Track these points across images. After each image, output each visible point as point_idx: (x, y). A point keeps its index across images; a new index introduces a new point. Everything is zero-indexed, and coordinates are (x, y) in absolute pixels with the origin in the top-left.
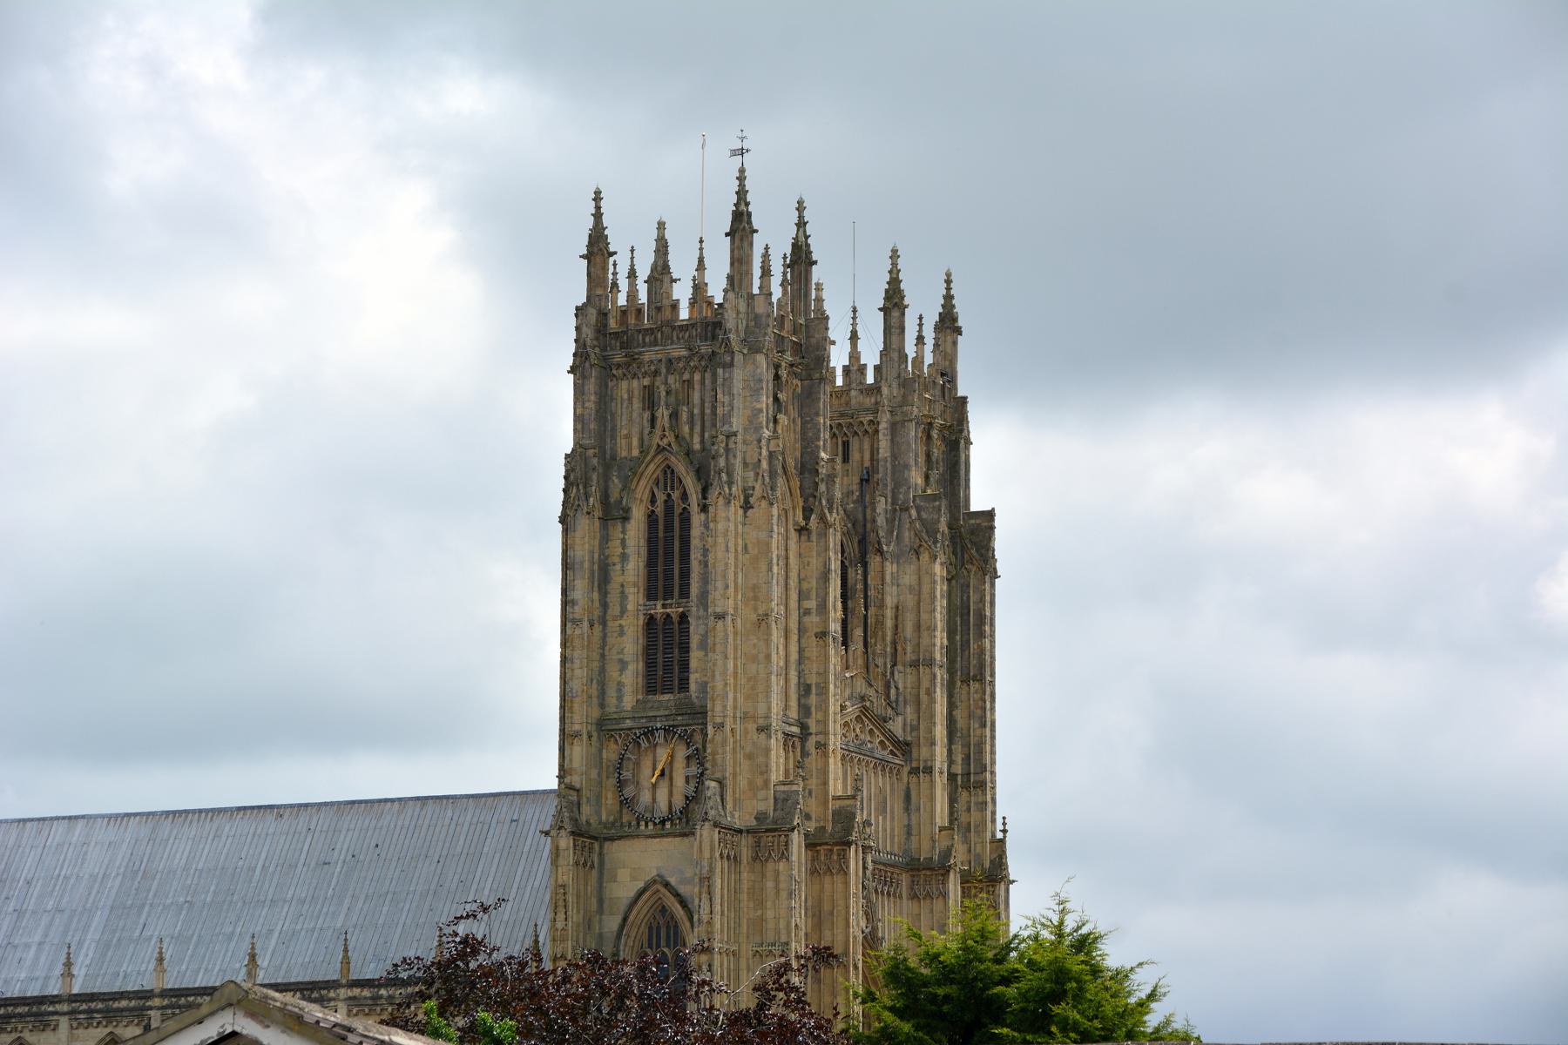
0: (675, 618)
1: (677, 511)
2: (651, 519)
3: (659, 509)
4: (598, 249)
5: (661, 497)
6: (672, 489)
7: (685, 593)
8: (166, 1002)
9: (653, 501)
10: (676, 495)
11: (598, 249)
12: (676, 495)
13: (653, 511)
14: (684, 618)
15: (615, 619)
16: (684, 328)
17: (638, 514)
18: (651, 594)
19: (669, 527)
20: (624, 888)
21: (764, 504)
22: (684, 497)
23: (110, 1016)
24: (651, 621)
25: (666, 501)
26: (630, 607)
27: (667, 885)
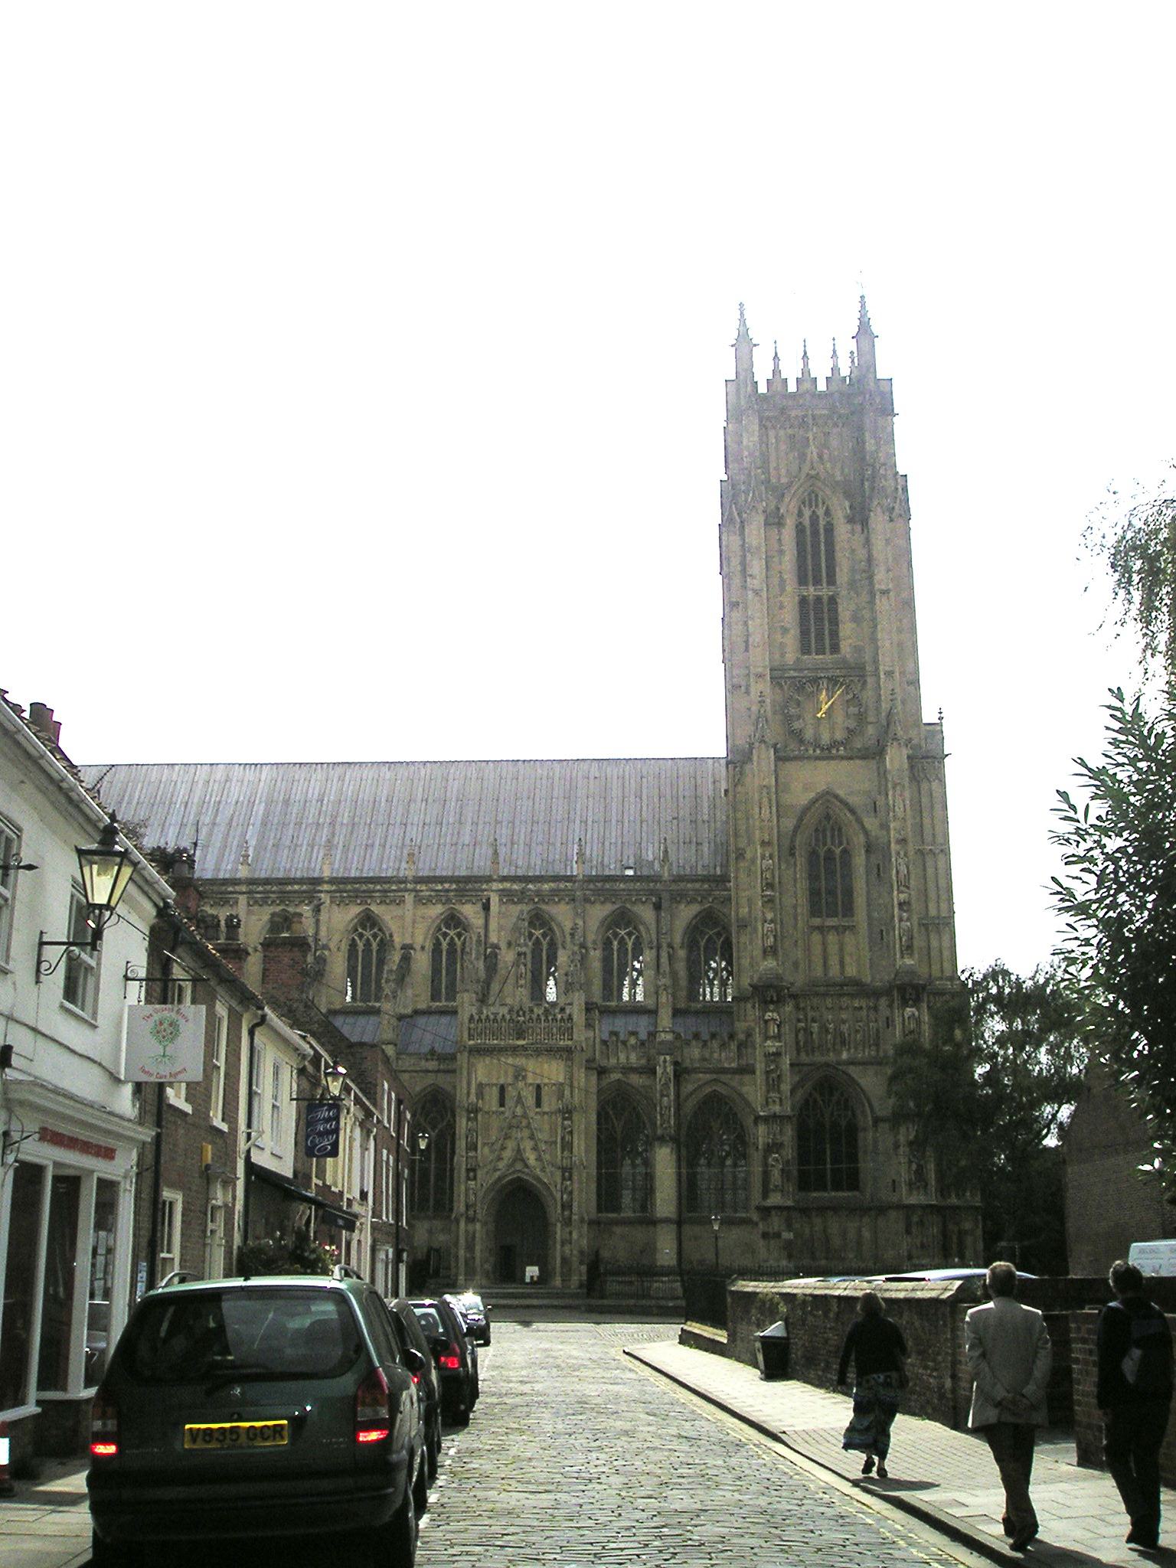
0: (825, 599)
1: (822, 523)
2: (800, 529)
3: (807, 522)
4: (744, 344)
5: (807, 513)
6: (817, 506)
7: (832, 580)
8: (334, 888)
9: (800, 514)
10: (821, 512)
11: (744, 344)
12: (821, 512)
13: (800, 523)
14: (833, 600)
15: (775, 597)
16: (822, 395)
17: (790, 522)
18: (802, 580)
19: (815, 533)
20: (799, 796)
21: (900, 520)
22: (827, 513)
23: (284, 897)
24: (803, 601)
25: (811, 517)
26: (789, 589)
27: (836, 797)
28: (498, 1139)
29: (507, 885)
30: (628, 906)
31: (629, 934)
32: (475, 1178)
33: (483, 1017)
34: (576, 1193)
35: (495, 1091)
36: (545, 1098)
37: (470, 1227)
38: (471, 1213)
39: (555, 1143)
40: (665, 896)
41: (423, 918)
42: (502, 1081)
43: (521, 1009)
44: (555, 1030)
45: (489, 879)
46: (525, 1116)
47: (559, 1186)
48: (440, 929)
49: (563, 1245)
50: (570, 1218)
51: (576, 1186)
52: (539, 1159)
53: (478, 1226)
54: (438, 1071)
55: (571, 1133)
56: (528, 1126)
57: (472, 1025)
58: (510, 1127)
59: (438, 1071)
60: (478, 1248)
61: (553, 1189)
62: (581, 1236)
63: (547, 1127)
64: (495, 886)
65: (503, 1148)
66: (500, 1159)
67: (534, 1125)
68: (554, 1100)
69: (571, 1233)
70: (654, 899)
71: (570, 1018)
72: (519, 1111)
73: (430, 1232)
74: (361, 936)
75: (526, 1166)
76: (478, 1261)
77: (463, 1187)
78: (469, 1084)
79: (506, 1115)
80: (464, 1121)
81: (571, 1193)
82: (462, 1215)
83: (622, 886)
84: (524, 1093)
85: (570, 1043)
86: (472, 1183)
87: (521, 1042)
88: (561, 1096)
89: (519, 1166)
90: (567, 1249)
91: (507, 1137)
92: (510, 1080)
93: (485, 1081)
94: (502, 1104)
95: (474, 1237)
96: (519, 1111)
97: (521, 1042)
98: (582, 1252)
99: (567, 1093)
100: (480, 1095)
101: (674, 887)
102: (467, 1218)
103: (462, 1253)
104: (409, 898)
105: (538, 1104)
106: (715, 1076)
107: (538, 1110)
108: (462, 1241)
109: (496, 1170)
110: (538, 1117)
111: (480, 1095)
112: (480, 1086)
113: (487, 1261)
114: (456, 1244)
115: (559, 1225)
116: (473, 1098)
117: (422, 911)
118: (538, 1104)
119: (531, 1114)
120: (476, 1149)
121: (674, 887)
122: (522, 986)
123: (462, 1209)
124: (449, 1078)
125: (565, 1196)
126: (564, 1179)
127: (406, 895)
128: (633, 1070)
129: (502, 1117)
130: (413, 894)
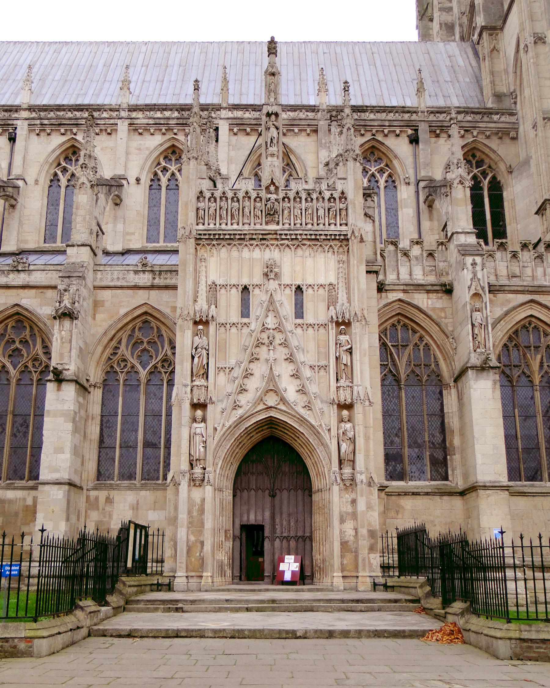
28: (239, 363)
29: (239, 114)
30: (380, 137)
31: (381, 171)
32: (204, 420)
33: (218, 194)
34: (360, 442)
35: (235, 295)
36: (308, 306)
37: (197, 494)
38: (198, 470)
39: (325, 367)
40: (423, 129)
41: (139, 149)
42: (245, 281)
43: (273, 183)
44: (321, 212)
45: (218, 108)
46: (279, 329)
47: (334, 432)
48: (159, 164)
49: (342, 521)
50: (353, 479)
51: (360, 430)
52: (302, 391)
53: (209, 489)
54: (152, 287)
55: (350, 351)
56: (285, 344)
57: (201, 205)
58: (259, 344)
59: (152, 287)
60: (208, 525)
61: (325, 436)
62: (369, 507)
63: (312, 346)
64: (224, 113)
65: (248, 375)
66: (243, 390)
67: (294, 342)
68: (322, 307)
69: (354, 502)
70: (410, 132)
71: (343, 196)
72: (271, 322)
73: (135, 508)
74: (65, 170)
75: (283, 400)
76: (208, 547)
77: (185, 433)
78: (197, 283)
79: (253, 327)
80: (189, 334)
81: (353, 441)
82: (183, 473)
83: (372, 116)
84: (277, 297)
85: (344, 228)
86: (199, 427)
87: (273, 227)
88: (332, 302)
89: (272, 400)
90: (349, 526)
91: (254, 359)
92: (258, 279)
93: (220, 281)
94: (245, 312)
95: (202, 511)
96: (271, 322)
97: (273, 227)
98: (372, 534)
99: (342, 296)
100: (213, 300)
101: (432, 118)
102: (192, 480)
103: (182, 533)
104: (123, 127)
105: (299, 313)
106: (528, 297)
107: (299, 321)
108: (183, 516)
109: (236, 406)
110: (299, 331)
111: (213, 300)
112: (213, 288)
113: (220, 546)
114: (174, 521)
115: (336, 488)
116: (202, 304)
117: (137, 141)
118: (299, 313)
119: (289, 326)
120: (206, 375)
121: (432, 118)
122: (272, 155)
123: (185, 466)
124: (165, 295)
125: (344, 447)
126: (341, 420)
127: (119, 122)
128: (419, 287)
129: (245, 330)
130: (127, 122)
